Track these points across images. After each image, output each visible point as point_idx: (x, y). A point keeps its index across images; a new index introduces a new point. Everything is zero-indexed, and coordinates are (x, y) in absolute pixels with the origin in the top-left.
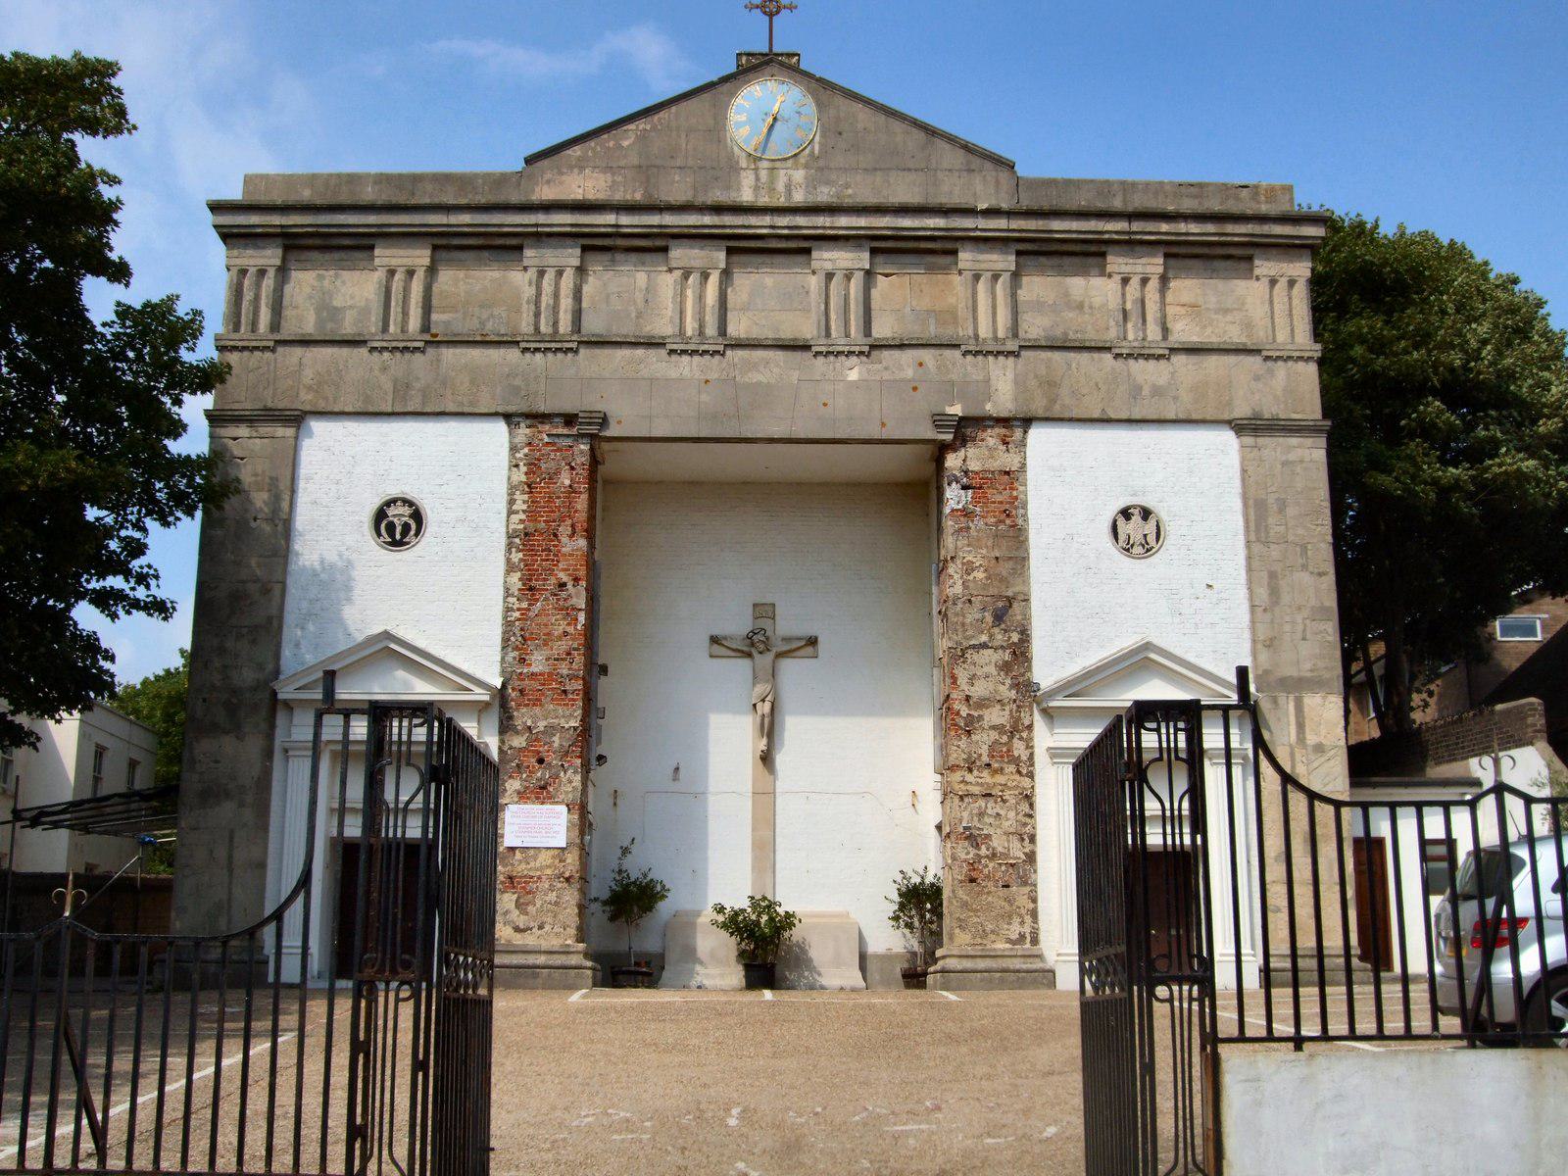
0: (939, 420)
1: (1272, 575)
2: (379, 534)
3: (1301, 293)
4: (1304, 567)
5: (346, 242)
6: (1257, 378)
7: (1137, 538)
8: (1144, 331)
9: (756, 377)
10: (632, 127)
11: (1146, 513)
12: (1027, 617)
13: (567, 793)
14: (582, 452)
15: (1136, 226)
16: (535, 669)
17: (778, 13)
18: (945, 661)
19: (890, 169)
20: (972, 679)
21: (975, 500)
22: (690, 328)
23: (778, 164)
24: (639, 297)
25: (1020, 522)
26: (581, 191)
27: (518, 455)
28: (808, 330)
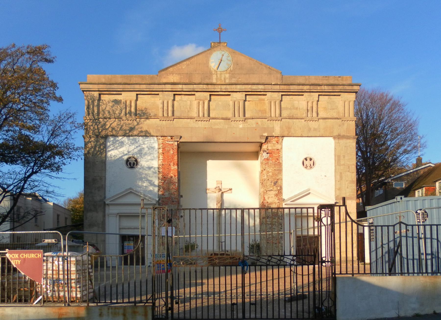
0: (261, 136)
1: (341, 173)
2: (127, 165)
3: (352, 104)
4: (349, 171)
5: (115, 93)
6: (340, 126)
7: (309, 165)
8: (312, 114)
9: (217, 127)
10: (185, 63)
11: (311, 159)
12: (282, 183)
13: (174, 224)
14: (175, 145)
15: (312, 87)
16: (166, 196)
17: (222, 32)
18: (262, 194)
19: (250, 74)
20: (269, 198)
21: (270, 156)
22: (201, 114)
23: (222, 73)
24: (188, 107)
25: (281, 161)
26: (173, 80)
27: (160, 146)
28: (229, 114)
